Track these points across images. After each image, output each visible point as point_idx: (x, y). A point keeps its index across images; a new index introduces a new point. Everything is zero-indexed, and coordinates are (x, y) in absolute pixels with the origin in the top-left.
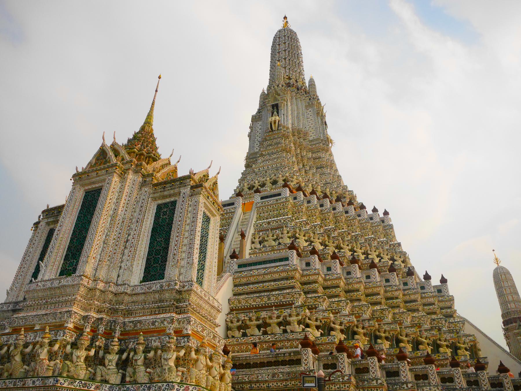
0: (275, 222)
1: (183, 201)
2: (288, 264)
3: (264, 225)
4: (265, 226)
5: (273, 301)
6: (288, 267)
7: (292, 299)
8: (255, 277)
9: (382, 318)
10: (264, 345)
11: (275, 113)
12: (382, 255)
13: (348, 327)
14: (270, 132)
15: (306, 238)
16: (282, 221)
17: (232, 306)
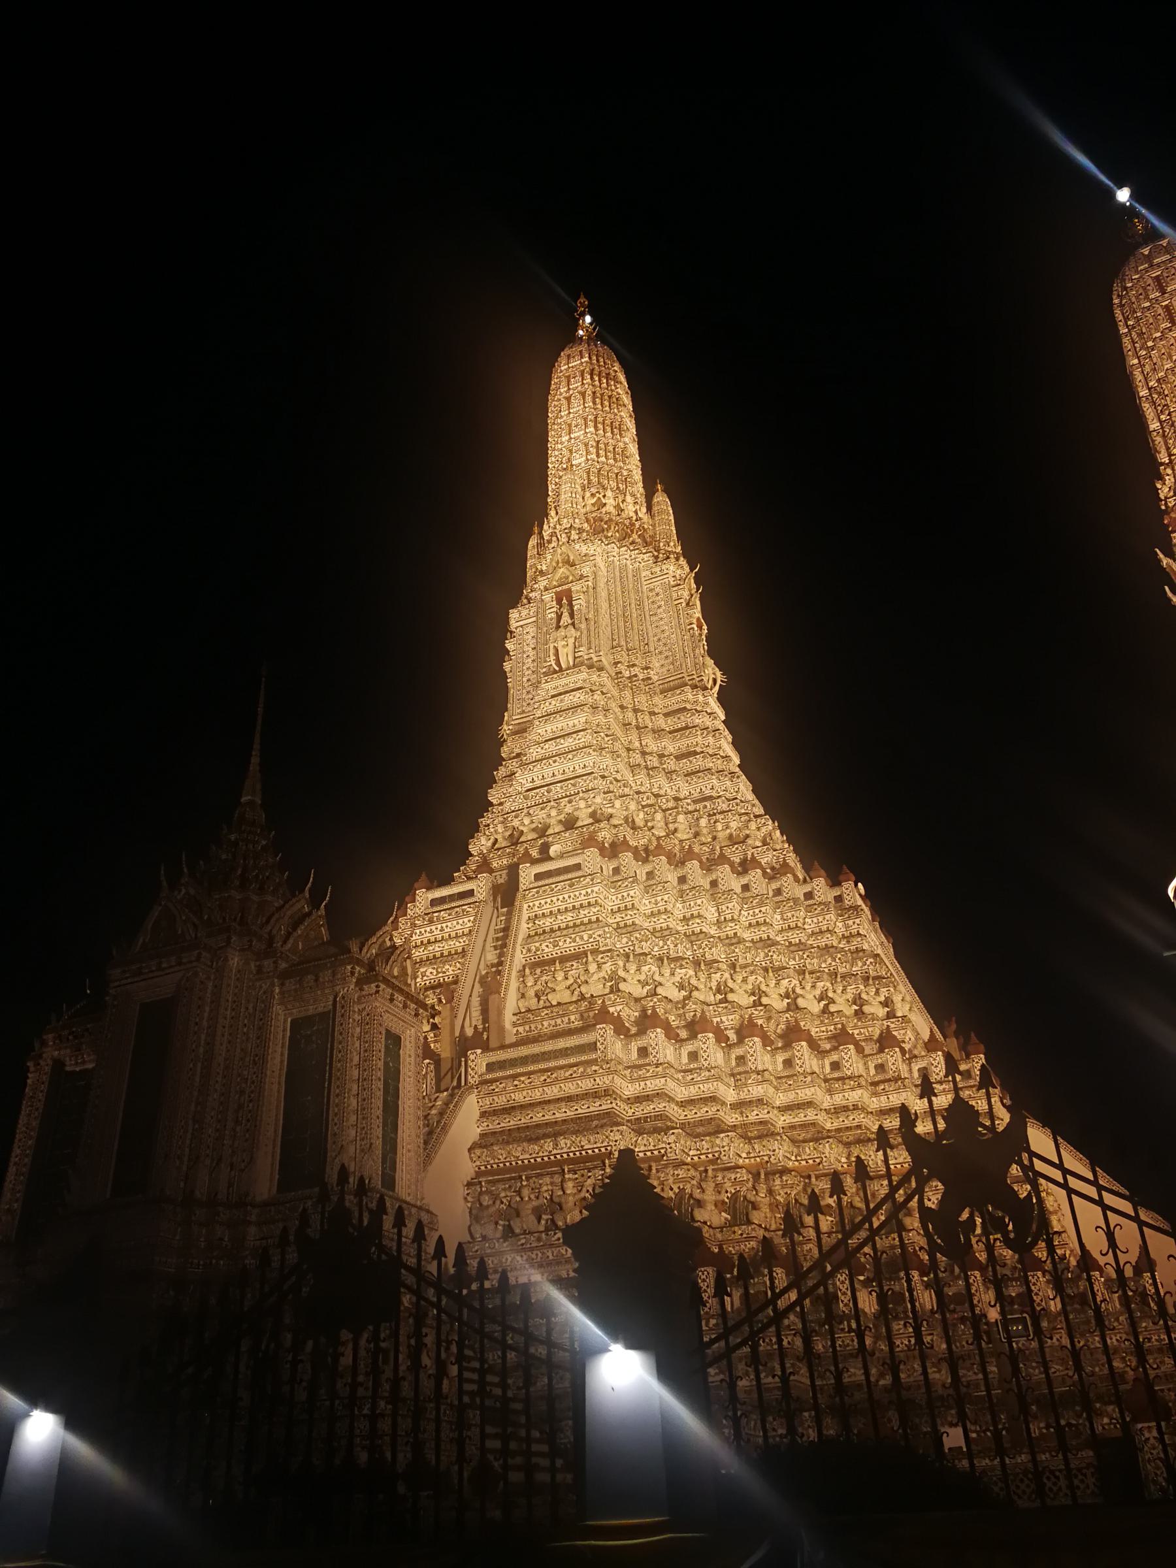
0: (568, 940)
1: (342, 1016)
2: (596, 1060)
3: (543, 947)
4: (547, 950)
5: (565, 1150)
6: (594, 1068)
7: (605, 1144)
8: (525, 1093)
9: (818, 1160)
10: (550, 1254)
11: (566, 619)
12: (830, 994)
13: (733, 1195)
14: (555, 672)
15: (643, 977)
16: (586, 937)
17: (478, 1163)
